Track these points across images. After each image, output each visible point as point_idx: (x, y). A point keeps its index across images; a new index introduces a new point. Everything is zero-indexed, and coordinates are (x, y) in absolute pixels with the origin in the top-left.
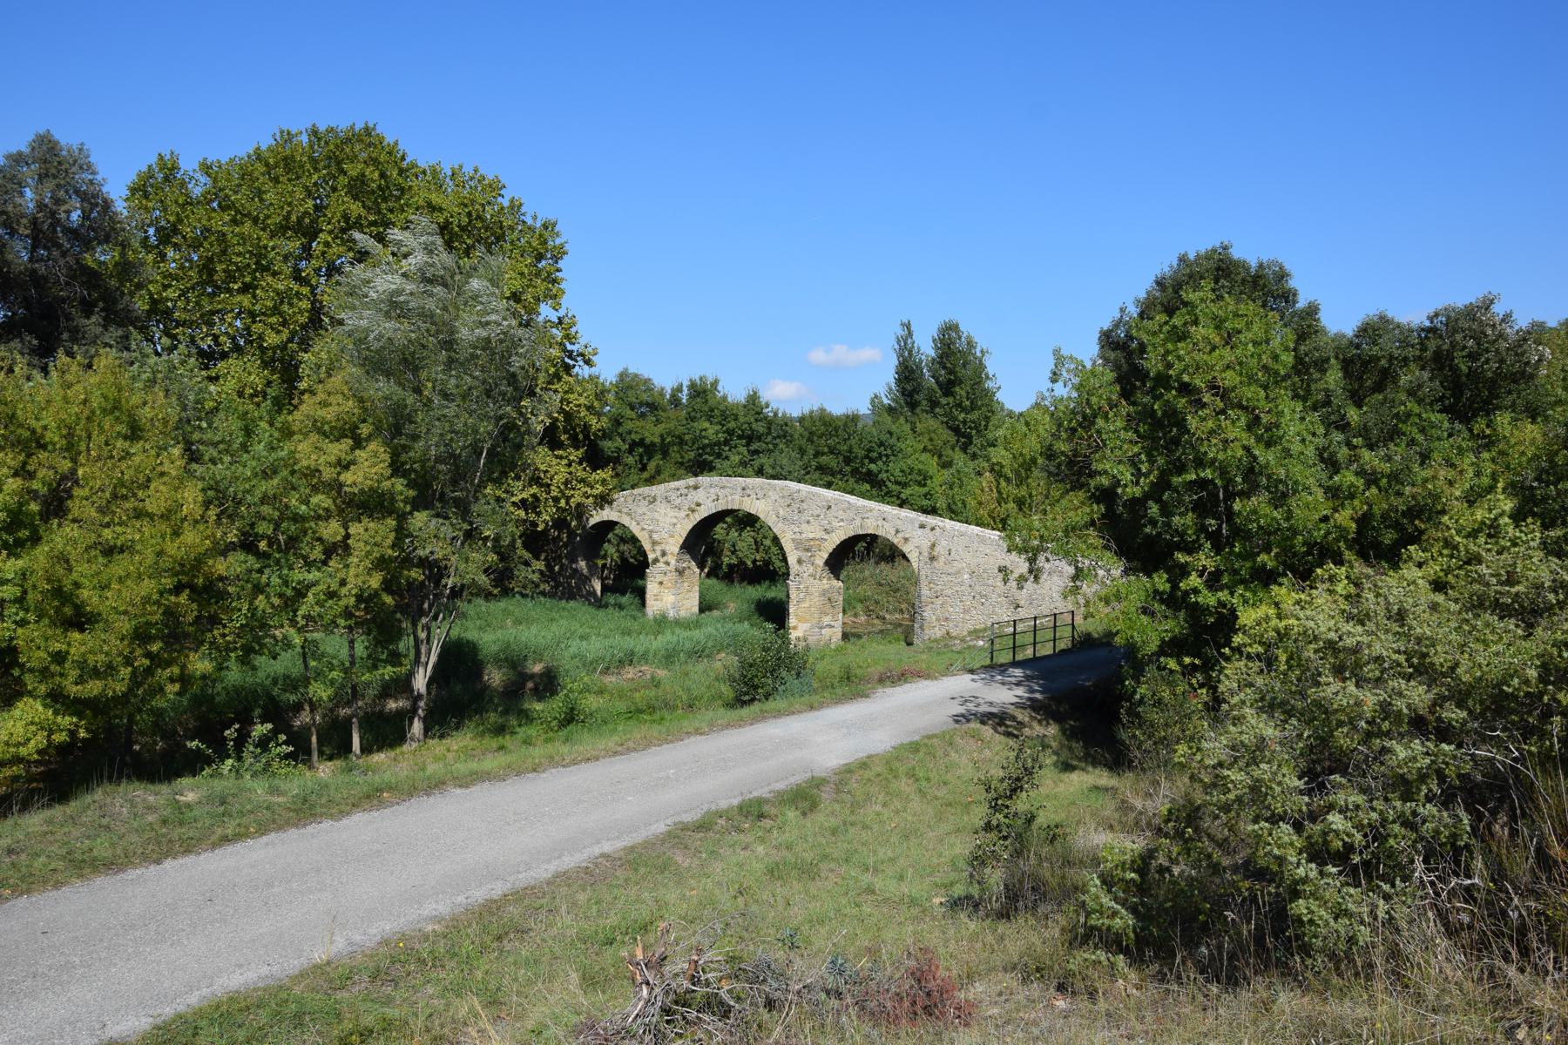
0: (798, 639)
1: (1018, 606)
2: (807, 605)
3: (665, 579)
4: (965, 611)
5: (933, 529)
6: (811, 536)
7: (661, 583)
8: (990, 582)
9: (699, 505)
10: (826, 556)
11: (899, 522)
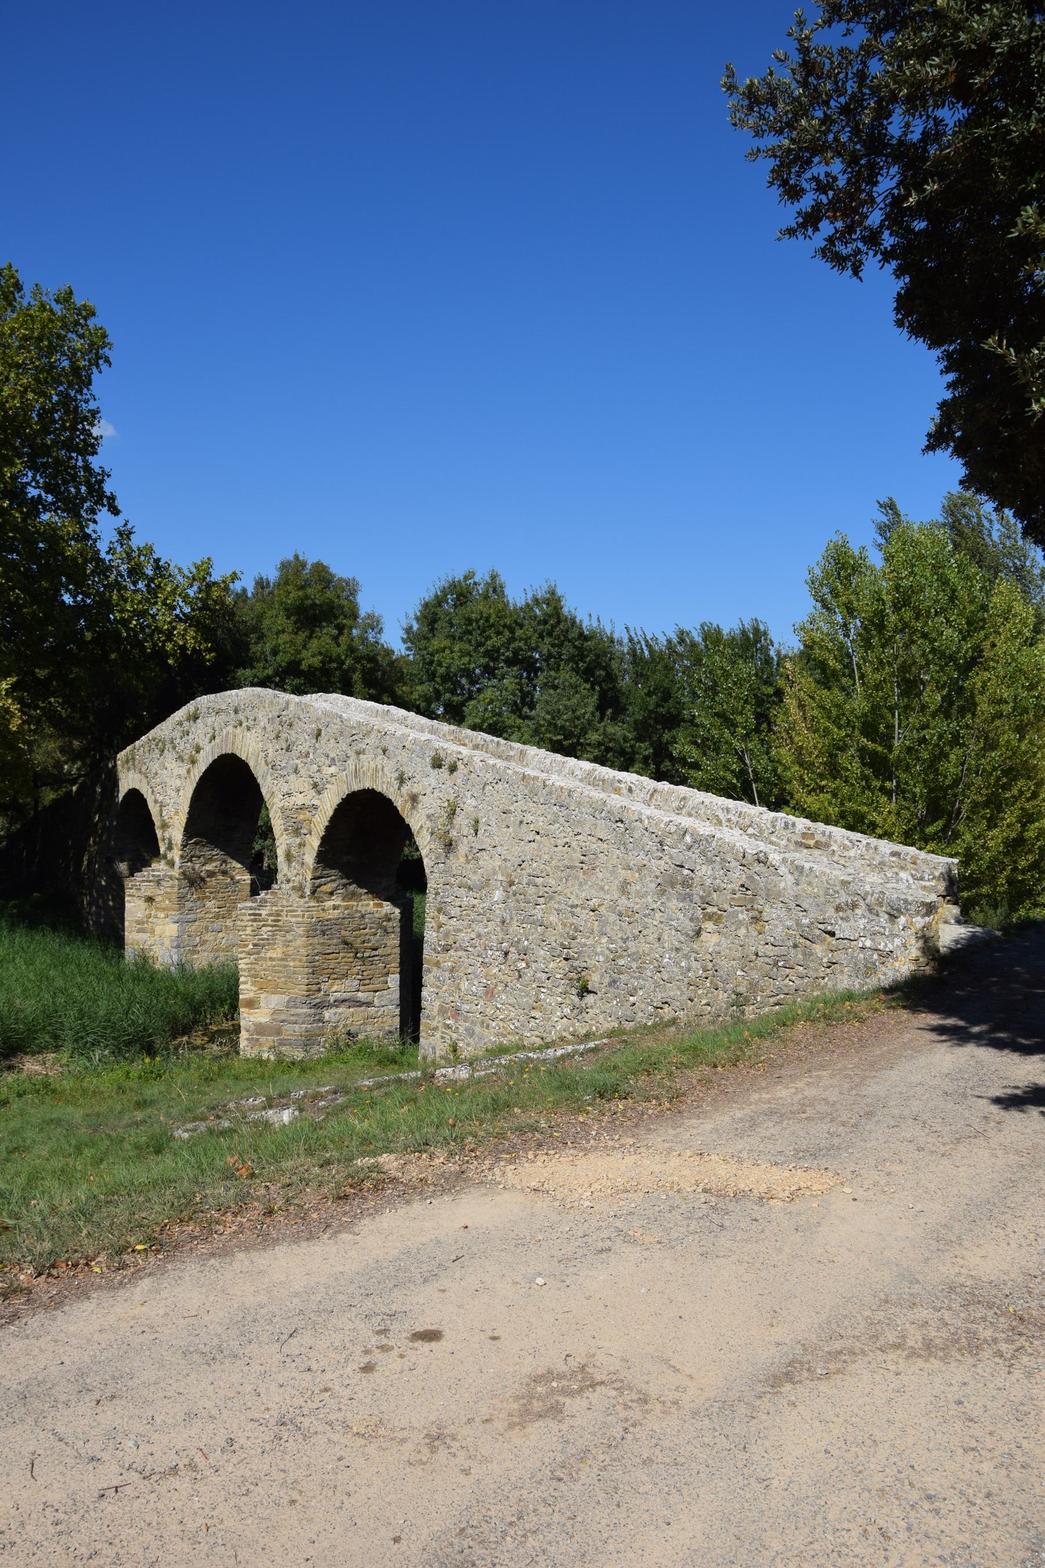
0: (261, 1030)
1: (584, 991)
2: (277, 953)
3: (159, 893)
4: (489, 993)
5: (453, 769)
6: (299, 800)
7: (150, 900)
8: (538, 913)
9: (198, 750)
10: (314, 842)
11: (403, 756)
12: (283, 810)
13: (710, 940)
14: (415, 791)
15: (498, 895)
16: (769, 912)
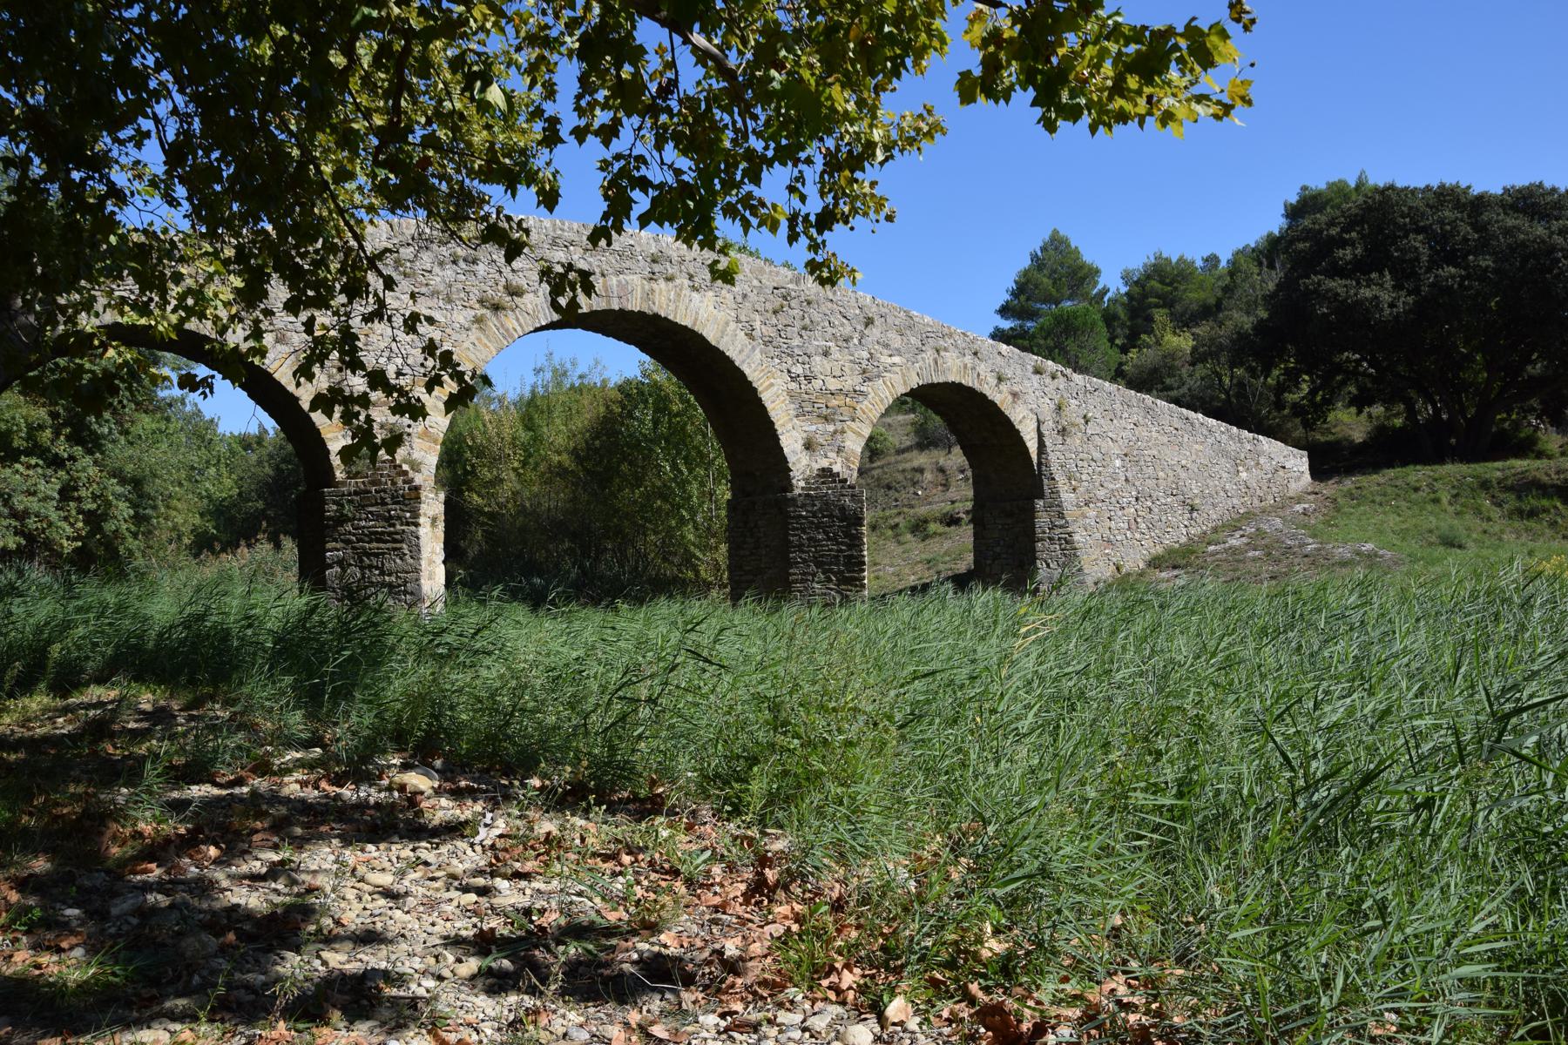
1: (1193, 509)
5: (1054, 378)
6: (833, 385)
12: (791, 396)
13: (1244, 475)
14: (1016, 388)
15: (1118, 463)
16: (1262, 461)
